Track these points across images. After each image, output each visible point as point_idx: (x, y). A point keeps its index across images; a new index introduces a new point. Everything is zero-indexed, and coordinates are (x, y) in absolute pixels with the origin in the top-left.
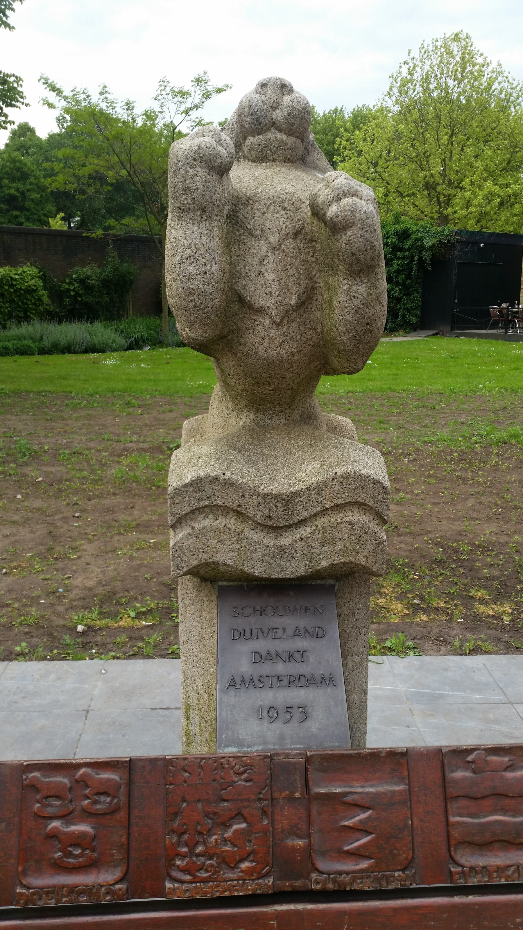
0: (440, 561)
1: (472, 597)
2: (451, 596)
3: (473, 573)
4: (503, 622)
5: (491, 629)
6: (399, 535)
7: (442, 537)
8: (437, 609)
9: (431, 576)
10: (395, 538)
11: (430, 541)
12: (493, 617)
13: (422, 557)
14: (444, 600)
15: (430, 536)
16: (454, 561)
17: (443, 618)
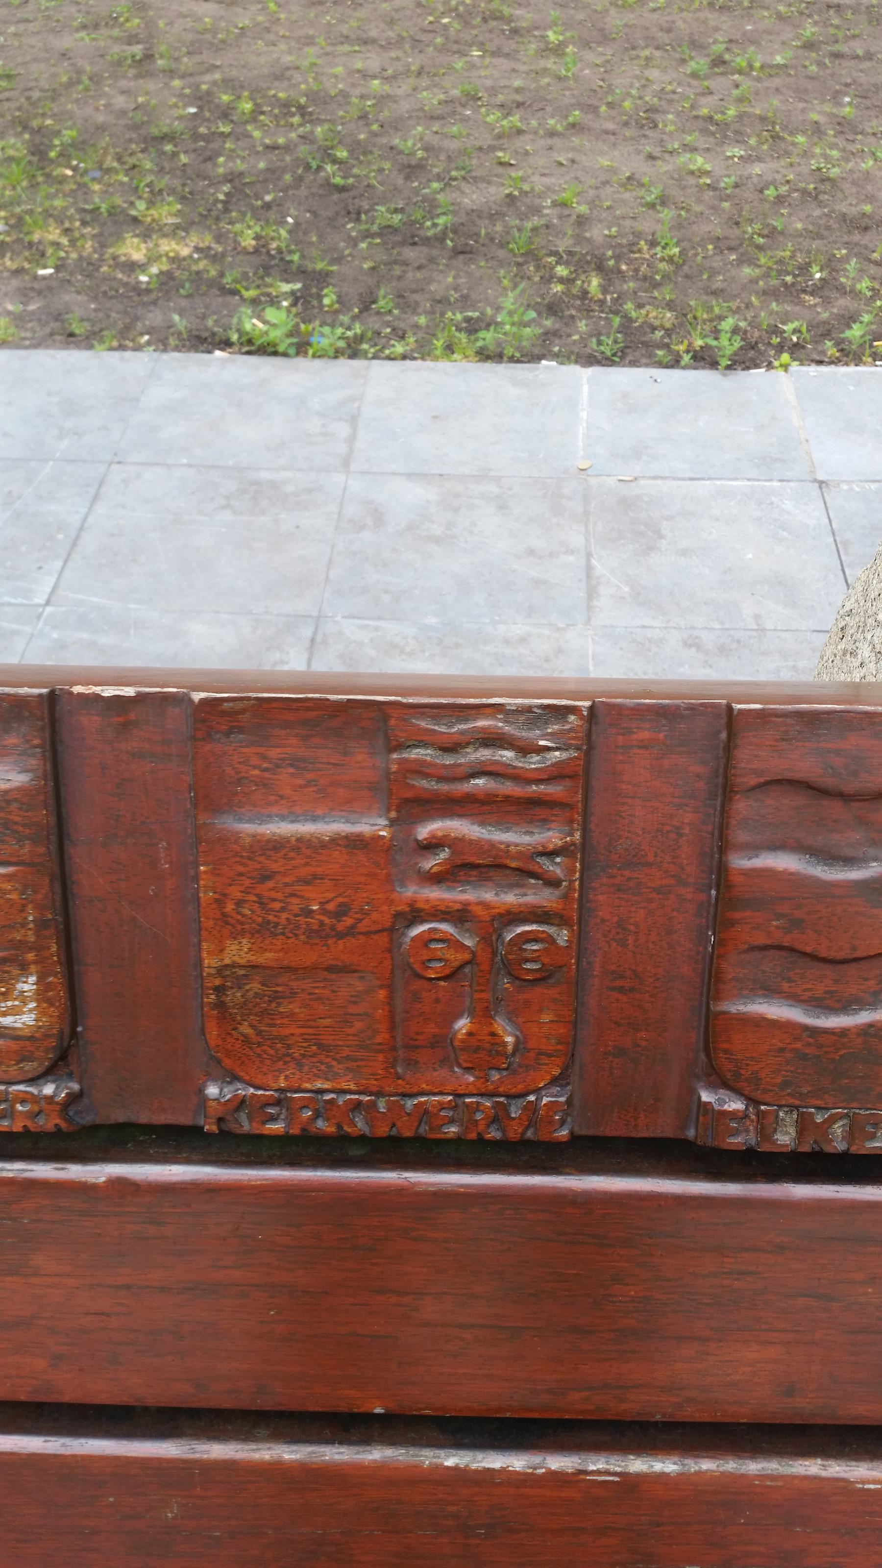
0: (165, 138)
1: (135, 220)
2: (91, 216)
3: (209, 165)
4: (137, 278)
5: (78, 293)
6: (137, 77)
7: (232, 80)
8: (31, 245)
9: (108, 171)
10: (123, 84)
11: (187, 91)
12: (132, 267)
13: (136, 127)
14: (67, 225)
15: (208, 78)
16: (196, 137)
17: (14, 267)
